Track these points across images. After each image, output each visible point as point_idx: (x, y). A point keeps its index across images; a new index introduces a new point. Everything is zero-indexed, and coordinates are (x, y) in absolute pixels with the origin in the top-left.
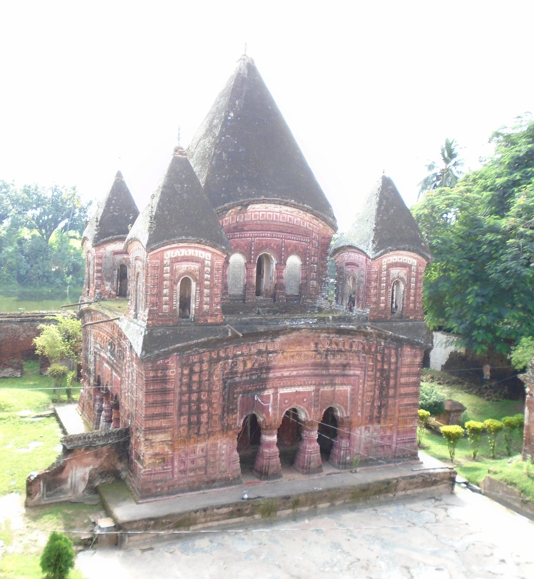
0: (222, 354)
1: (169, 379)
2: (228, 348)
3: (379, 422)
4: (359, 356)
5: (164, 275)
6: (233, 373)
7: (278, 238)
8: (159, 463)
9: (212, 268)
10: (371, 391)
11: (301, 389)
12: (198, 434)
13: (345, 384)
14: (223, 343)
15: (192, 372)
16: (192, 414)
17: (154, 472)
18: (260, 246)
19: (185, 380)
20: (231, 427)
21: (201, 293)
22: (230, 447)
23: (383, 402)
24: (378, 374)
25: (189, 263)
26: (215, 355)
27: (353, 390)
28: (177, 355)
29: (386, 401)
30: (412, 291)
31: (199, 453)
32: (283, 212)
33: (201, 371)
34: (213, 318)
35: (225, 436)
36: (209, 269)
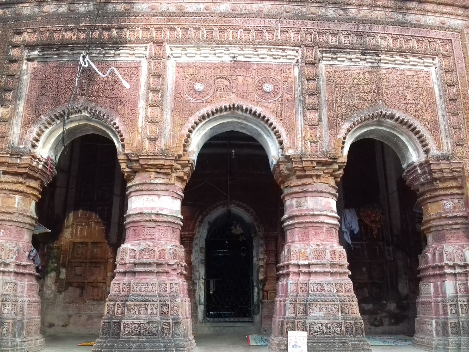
13: (413, 52)
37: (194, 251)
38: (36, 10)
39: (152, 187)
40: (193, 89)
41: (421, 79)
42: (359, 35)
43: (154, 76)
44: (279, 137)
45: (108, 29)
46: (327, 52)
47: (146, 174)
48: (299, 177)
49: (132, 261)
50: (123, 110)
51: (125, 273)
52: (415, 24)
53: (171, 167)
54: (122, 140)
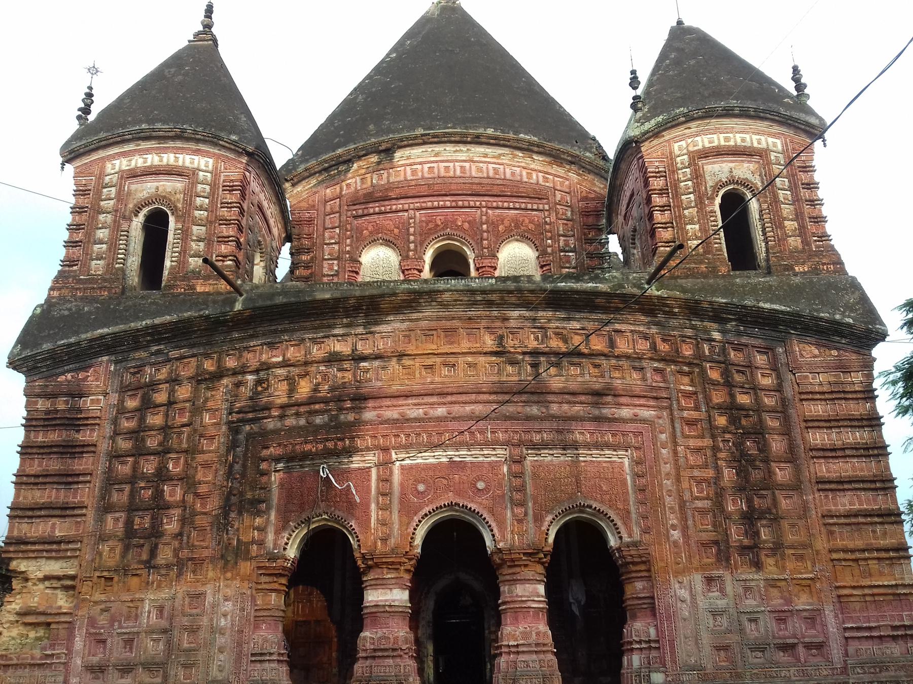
0: (231, 363)
1: (87, 418)
2: (246, 348)
3: (758, 565)
4: (642, 369)
5: (102, 203)
6: (258, 408)
7: (469, 207)
8: (38, 639)
9: (214, 185)
10: (706, 466)
11: (463, 455)
12: (149, 564)
13: (608, 446)
14: (231, 330)
15: (147, 405)
16: (137, 510)
17: (15, 662)
18: (431, 226)
19: (127, 424)
20: (248, 551)
21: (185, 234)
22: (242, 609)
23: (756, 501)
24: (722, 421)
25: (162, 177)
26: (212, 365)
27: (638, 462)
28: (110, 361)
29: (769, 500)
30: (787, 210)
31: (148, 616)
32: (476, 159)
33: (170, 403)
34: (211, 282)
35: (229, 575)
36: (208, 188)
37: (420, 626)
38: (279, 424)
39: (385, 582)
40: (416, 489)
41: (616, 470)
42: (559, 431)
43: (383, 481)
44: (492, 531)
45: (342, 440)
46: (532, 449)
47: (379, 570)
48: (510, 567)
49: (372, 647)
50: (358, 513)
51: (366, 658)
52: (609, 418)
53: (400, 563)
54: (358, 541)
